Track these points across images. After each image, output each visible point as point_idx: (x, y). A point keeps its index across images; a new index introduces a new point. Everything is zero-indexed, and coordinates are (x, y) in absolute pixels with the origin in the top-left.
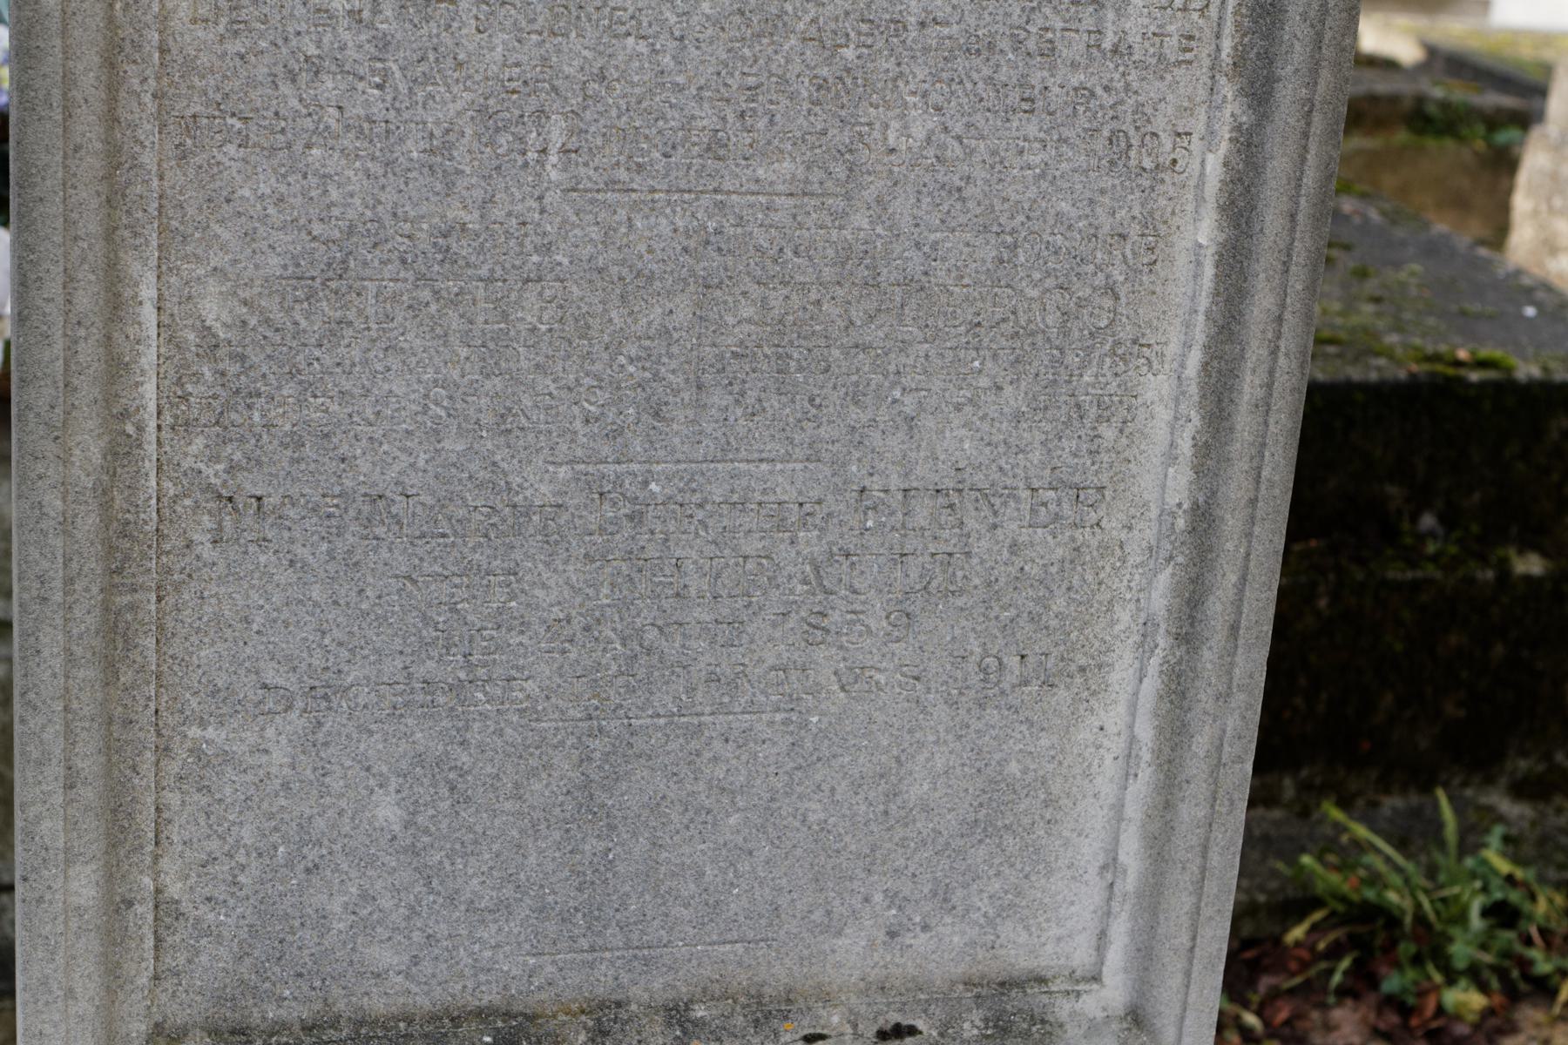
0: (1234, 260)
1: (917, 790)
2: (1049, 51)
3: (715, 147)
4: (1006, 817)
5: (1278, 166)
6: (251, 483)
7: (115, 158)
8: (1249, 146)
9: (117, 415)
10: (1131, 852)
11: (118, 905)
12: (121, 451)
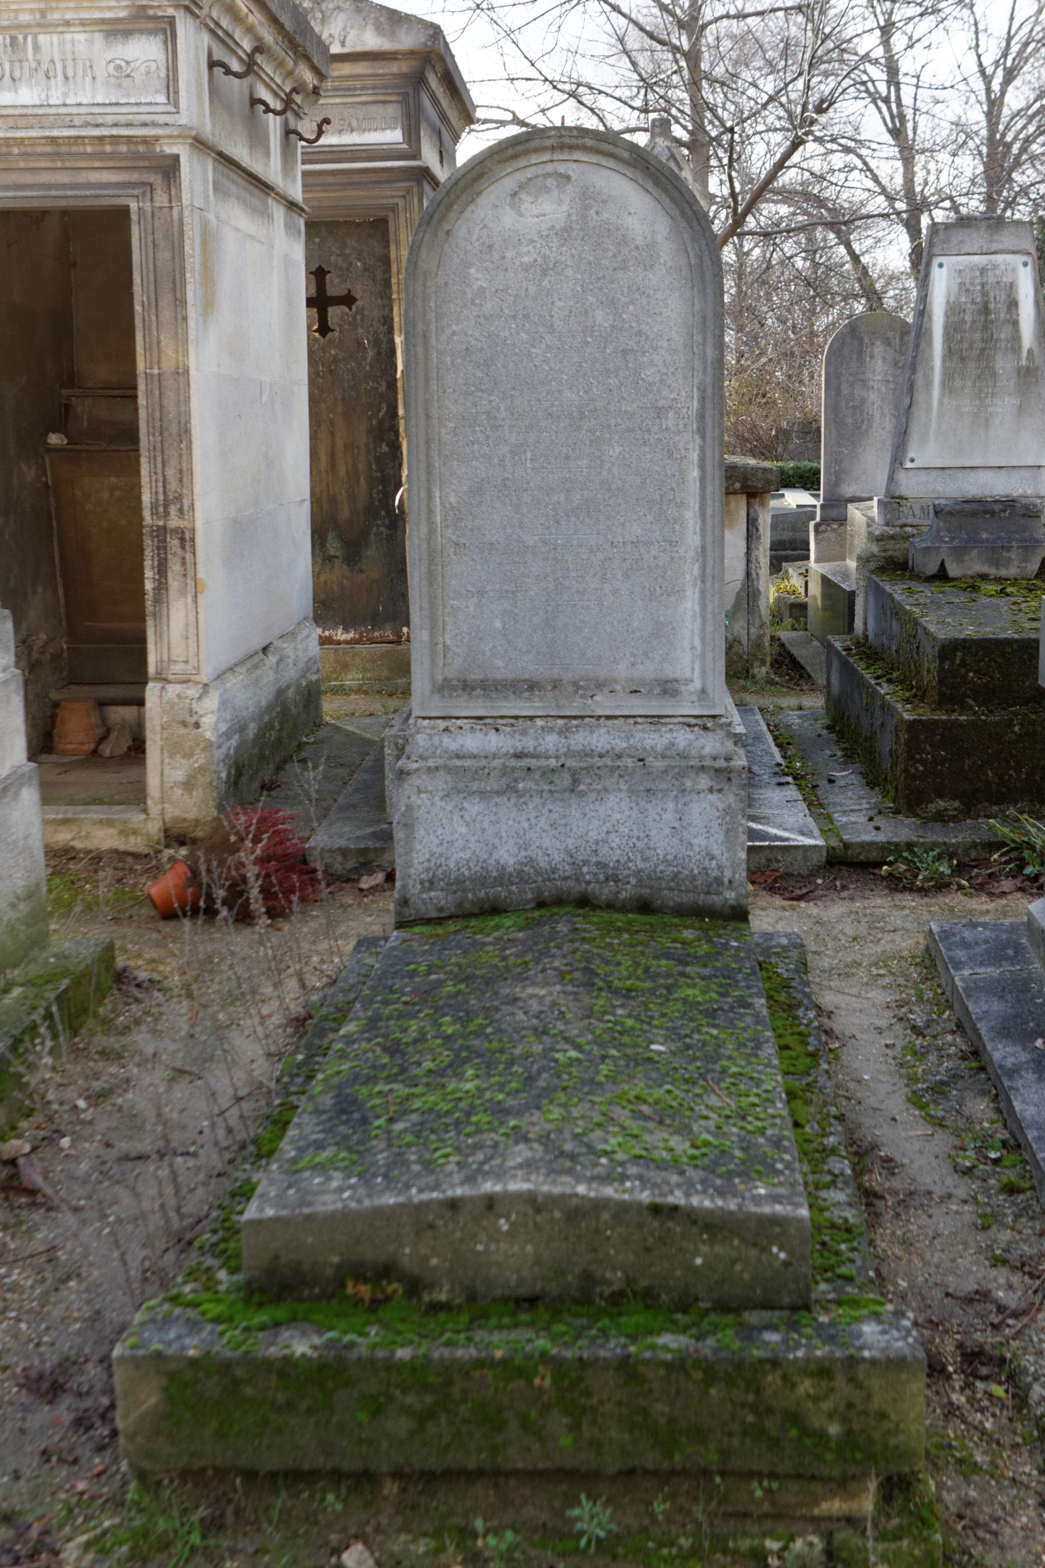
0: (703, 479)
1: (635, 624)
2: (649, 431)
3: (567, 458)
4: (661, 632)
5: (709, 454)
6: (462, 540)
7: (429, 465)
8: (702, 450)
9: (431, 523)
10: (697, 643)
11: (434, 644)
12: (432, 531)
